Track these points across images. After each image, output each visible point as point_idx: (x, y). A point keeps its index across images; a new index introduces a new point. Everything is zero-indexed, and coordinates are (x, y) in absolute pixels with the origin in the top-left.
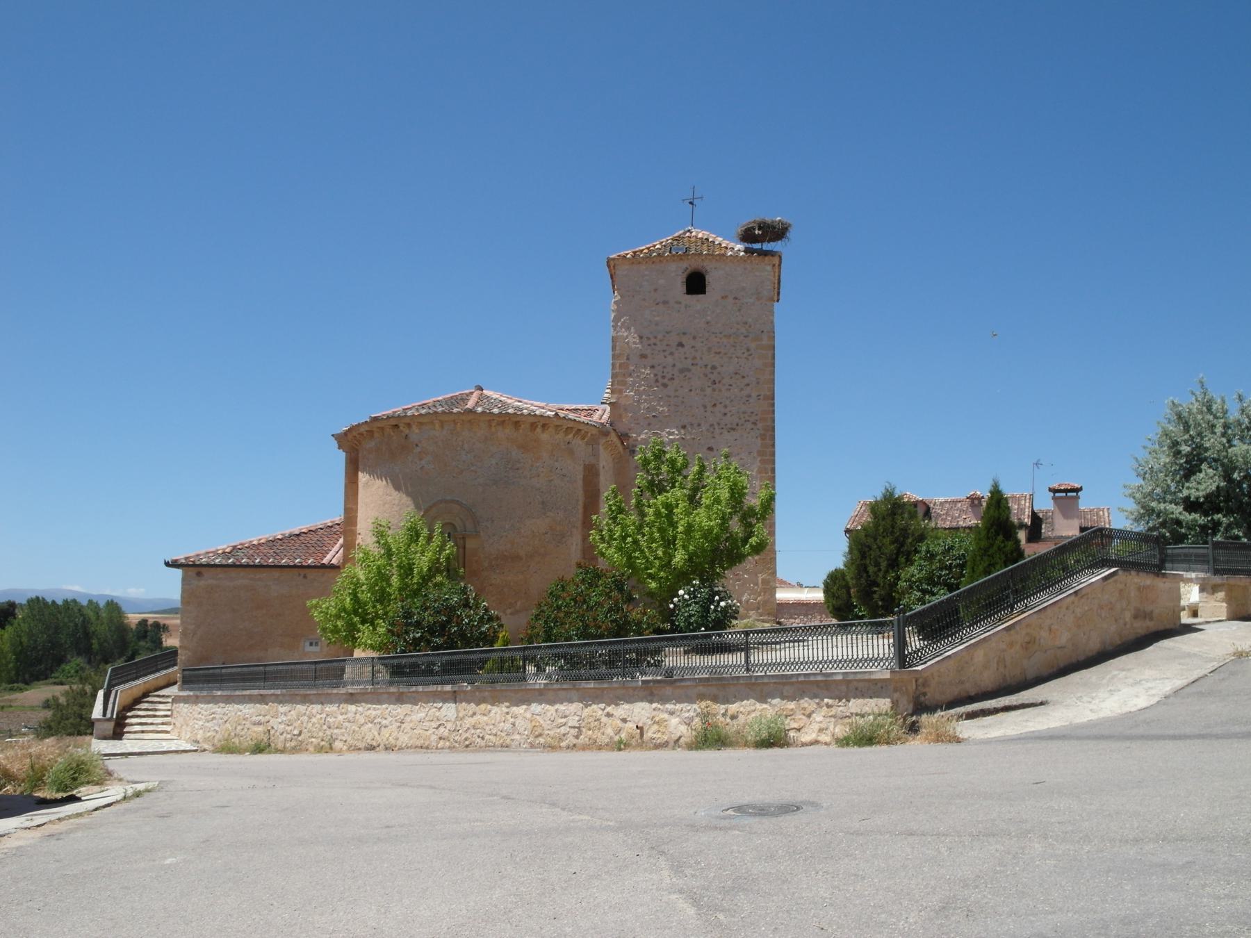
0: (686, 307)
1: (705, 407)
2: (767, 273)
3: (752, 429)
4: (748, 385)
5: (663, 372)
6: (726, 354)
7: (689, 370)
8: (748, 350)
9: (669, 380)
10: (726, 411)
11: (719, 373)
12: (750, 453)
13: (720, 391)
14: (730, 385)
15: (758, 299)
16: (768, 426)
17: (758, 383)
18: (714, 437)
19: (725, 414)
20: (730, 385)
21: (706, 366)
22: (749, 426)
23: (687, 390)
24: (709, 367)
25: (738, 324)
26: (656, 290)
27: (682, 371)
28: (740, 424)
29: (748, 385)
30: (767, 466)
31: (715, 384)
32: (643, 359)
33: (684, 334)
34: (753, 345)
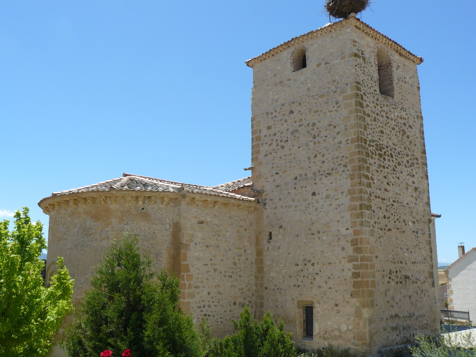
0: (294, 82)
1: (309, 158)
2: (347, 35)
3: (343, 171)
4: (339, 133)
5: (281, 137)
6: (321, 111)
7: (297, 131)
8: (337, 103)
9: (285, 142)
10: (324, 159)
11: (318, 128)
12: (342, 193)
13: (319, 143)
14: (326, 136)
15: (342, 58)
16: (355, 166)
17: (346, 129)
18: (315, 184)
19: (323, 162)
20: (326, 136)
21: (308, 124)
22: (341, 168)
23: (296, 148)
24: (310, 125)
25: (329, 83)
26: (275, 75)
27: (292, 133)
28: (334, 169)
29: (339, 133)
30: (356, 203)
31: (315, 138)
32: (269, 130)
33: (293, 103)
34: (340, 98)
